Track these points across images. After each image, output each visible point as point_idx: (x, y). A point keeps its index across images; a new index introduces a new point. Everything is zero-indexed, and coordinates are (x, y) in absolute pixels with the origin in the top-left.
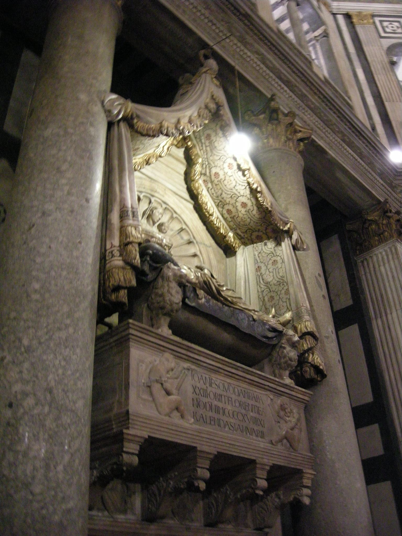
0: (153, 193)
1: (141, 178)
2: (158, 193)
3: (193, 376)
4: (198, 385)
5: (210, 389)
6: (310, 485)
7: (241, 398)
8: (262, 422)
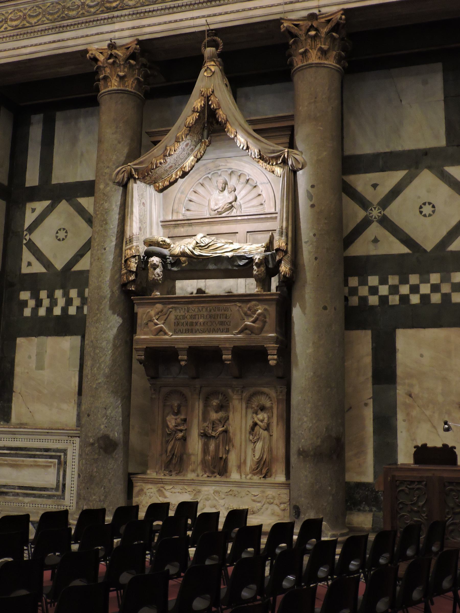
0: (218, 168)
1: (204, 165)
2: (222, 165)
3: (176, 310)
4: (179, 314)
5: (187, 314)
6: (276, 353)
7: (213, 313)
8: (228, 323)
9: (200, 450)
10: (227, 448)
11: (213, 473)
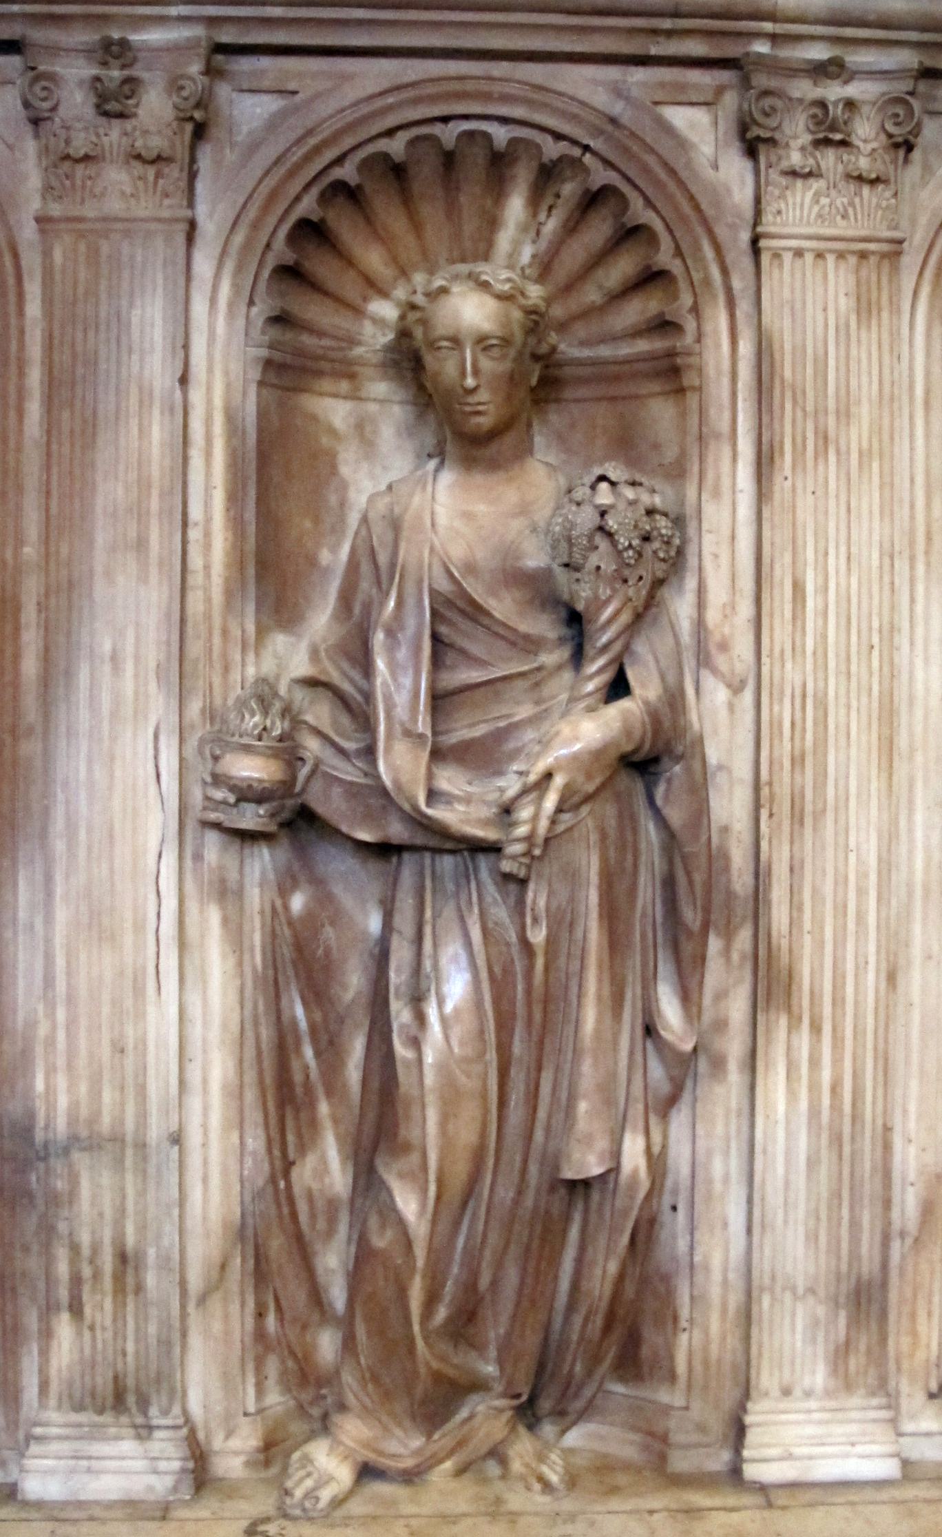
9: (217, 1068)
10: (670, 1010)
11: (437, 1402)
